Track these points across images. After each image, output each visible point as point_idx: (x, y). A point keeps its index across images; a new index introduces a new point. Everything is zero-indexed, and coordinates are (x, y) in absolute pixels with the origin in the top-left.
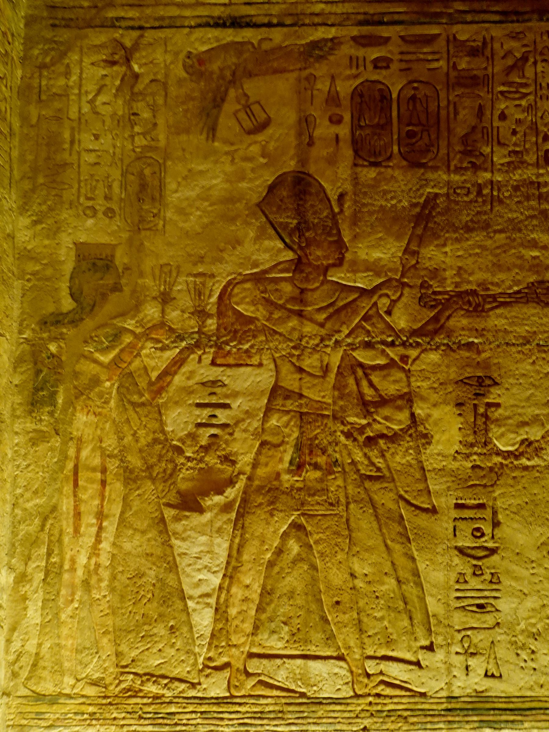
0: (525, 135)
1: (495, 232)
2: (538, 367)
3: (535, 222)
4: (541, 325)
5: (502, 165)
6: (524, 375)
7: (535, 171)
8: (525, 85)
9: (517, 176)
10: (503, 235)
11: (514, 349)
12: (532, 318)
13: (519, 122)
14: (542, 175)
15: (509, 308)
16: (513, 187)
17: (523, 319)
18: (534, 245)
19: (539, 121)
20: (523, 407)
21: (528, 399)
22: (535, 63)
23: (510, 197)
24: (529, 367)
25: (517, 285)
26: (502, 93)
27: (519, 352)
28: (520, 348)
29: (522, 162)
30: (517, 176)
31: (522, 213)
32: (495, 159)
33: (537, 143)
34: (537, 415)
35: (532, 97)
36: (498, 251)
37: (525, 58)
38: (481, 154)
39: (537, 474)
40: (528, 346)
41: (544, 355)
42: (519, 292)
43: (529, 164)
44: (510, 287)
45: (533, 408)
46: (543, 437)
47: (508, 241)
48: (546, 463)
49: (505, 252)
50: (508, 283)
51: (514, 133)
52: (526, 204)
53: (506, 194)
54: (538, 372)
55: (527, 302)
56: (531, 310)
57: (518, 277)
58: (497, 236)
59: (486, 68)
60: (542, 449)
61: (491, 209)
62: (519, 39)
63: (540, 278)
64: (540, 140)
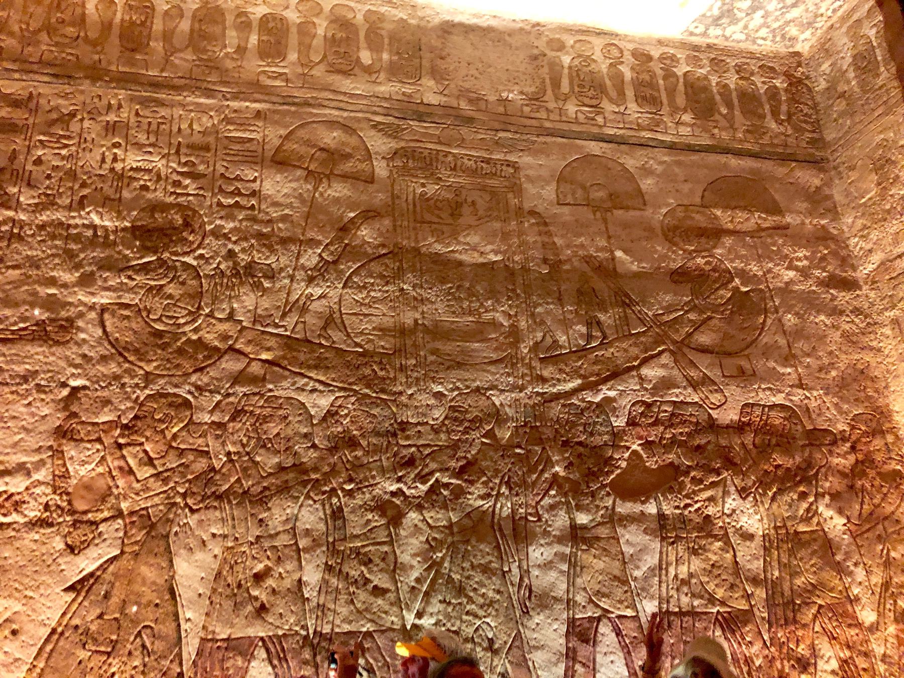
0: (61, 179)
1: (8, 268)
2: (33, 409)
3: (57, 261)
4: (46, 363)
5: (29, 205)
6: (14, 417)
7: (66, 214)
8: (69, 138)
9: (44, 217)
10: (18, 272)
11: (7, 389)
12: (36, 357)
13: (56, 168)
14: (74, 217)
15: (9, 345)
16: (37, 226)
17: (26, 357)
18: (52, 282)
19: (79, 170)
20: (8, 454)
21: (15, 445)
22: (82, 120)
23: (33, 235)
24: (22, 409)
25: (25, 322)
26: (41, 141)
27: (12, 393)
28: (14, 389)
29: (53, 205)
30: (44, 217)
31: (44, 252)
32: (22, 199)
33: (71, 188)
34: (24, 463)
35: (74, 148)
36: (8, 287)
37: (73, 115)
38: (6, 193)
39: (13, 534)
40: (25, 386)
41: (43, 396)
42: (25, 329)
43: (60, 206)
44: (15, 324)
45: (19, 455)
46: (27, 489)
47: (23, 277)
48: (26, 519)
49: (15, 288)
50: (12, 320)
51: (49, 177)
52: (50, 243)
53: (29, 232)
54: (33, 415)
55: (33, 340)
56: (36, 350)
57: (27, 314)
58: (10, 271)
59: (26, 119)
60: (24, 502)
61: (8, 246)
62: (67, 99)
63: (53, 316)
64: (76, 187)
